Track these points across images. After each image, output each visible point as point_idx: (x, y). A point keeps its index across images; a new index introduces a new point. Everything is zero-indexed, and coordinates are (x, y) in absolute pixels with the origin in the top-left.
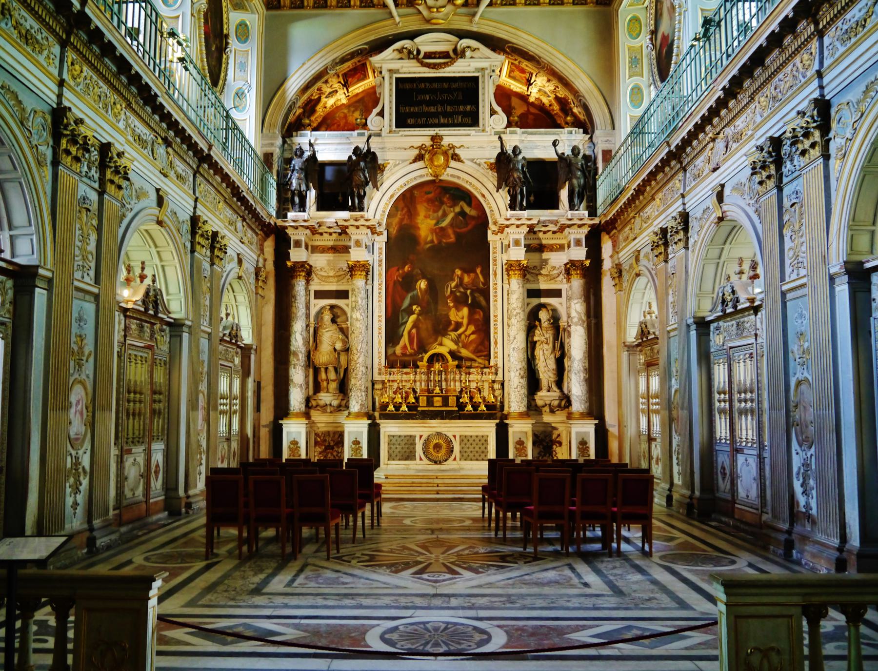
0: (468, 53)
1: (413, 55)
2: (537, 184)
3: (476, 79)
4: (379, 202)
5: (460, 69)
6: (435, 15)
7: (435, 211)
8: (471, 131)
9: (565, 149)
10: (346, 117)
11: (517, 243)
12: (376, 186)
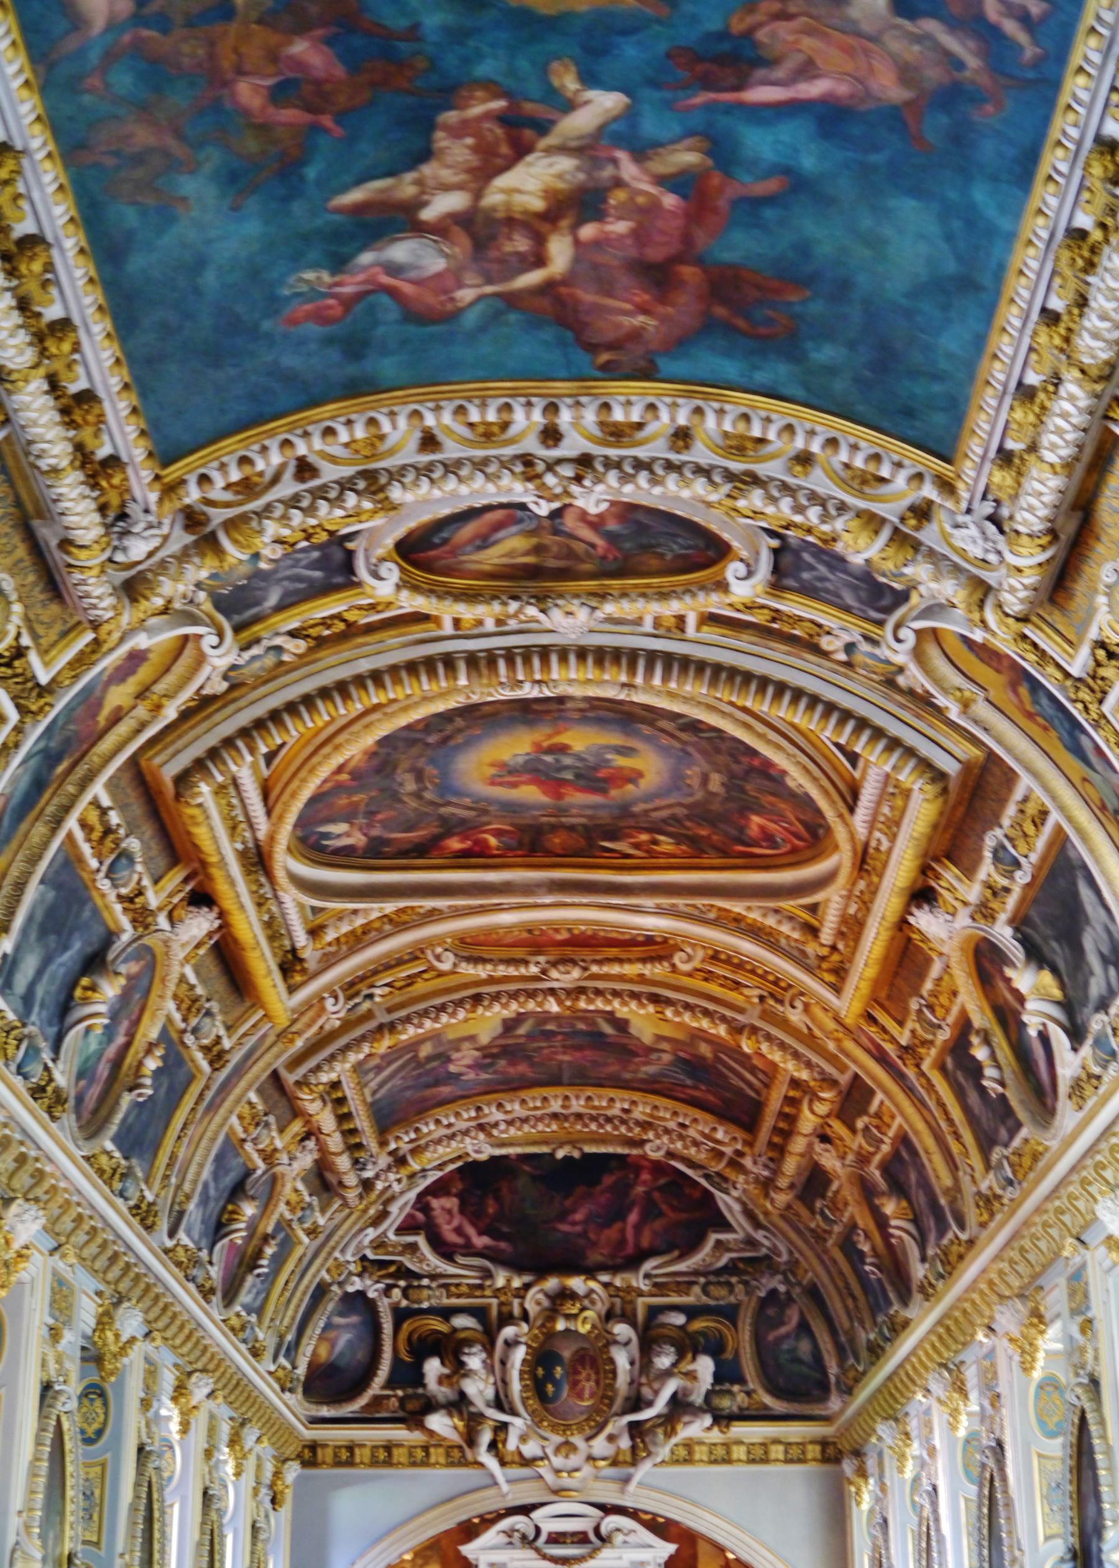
0: (619, 1538)
6: (565, 1481)
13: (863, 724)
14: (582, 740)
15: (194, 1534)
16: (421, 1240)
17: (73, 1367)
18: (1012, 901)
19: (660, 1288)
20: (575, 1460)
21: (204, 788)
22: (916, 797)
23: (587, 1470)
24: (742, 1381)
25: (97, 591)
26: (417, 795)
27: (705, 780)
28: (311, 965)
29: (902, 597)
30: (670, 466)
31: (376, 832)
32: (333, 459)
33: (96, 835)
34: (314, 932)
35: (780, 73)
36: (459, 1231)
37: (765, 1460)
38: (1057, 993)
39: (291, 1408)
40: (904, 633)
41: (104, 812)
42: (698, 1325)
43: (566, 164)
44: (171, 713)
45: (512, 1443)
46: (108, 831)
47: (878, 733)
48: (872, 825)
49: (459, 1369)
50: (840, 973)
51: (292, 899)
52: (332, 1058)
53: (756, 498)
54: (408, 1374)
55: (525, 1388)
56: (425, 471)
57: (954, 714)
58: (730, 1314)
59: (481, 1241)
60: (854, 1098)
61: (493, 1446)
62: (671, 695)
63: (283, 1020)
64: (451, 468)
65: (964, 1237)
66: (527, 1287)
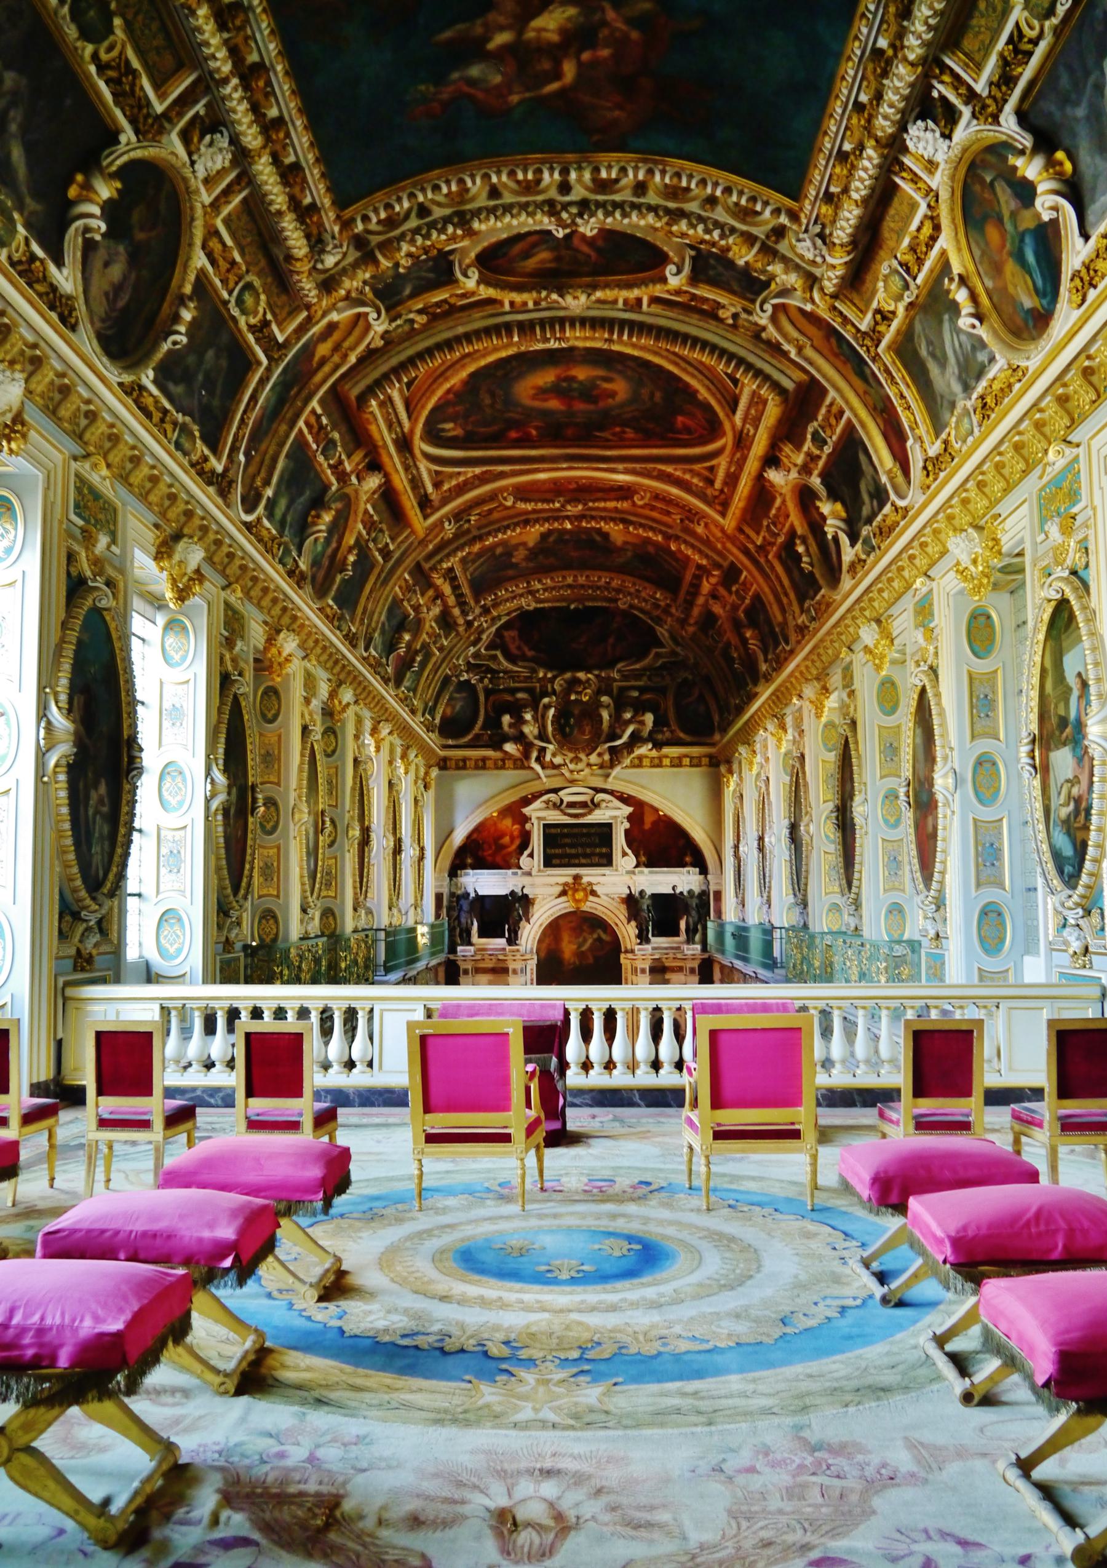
0: (604, 805)
1: (557, 806)
2: (662, 915)
3: (610, 825)
4: (530, 933)
5: (597, 817)
6: (576, 776)
7: (577, 937)
8: (606, 870)
9: (683, 888)
10: (495, 824)
11: (643, 971)
12: (528, 921)
13: (741, 361)
14: (582, 373)
15: (385, 801)
16: (498, 653)
17: (318, 718)
18: (821, 463)
19: (625, 678)
20: (580, 766)
21: (373, 403)
22: (770, 403)
23: (587, 771)
24: (668, 725)
25: (308, 287)
26: (492, 406)
27: (652, 395)
28: (436, 503)
29: (766, 285)
30: (634, 206)
31: (469, 428)
32: (439, 204)
33: (315, 430)
34: (437, 485)
36: (519, 648)
37: (680, 765)
38: (844, 514)
39: (432, 739)
40: (768, 307)
41: (318, 417)
42: (647, 696)
44: (353, 359)
45: (548, 758)
46: (321, 427)
47: (749, 367)
48: (745, 420)
49: (519, 721)
50: (724, 507)
51: (424, 466)
52: (448, 556)
53: (683, 225)
54: (493, 722)
55: (554, 730)
56: (492, 211)
57: (793, 355)
58: (662, 691)
59: (530, 653)
60: (731, 575)
61: (538, 760)
62: (634, 346)
63: (421, 533)
64: (508, 209)
65: (788, 648)
66: (555, 677)
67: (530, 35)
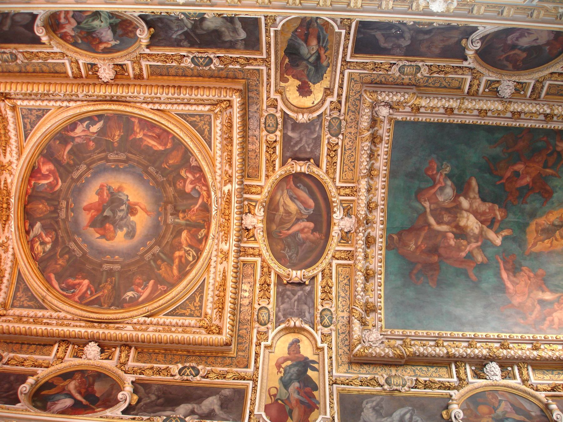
35: (512, 278)
43: (477, 231)
67: (465, 214)
